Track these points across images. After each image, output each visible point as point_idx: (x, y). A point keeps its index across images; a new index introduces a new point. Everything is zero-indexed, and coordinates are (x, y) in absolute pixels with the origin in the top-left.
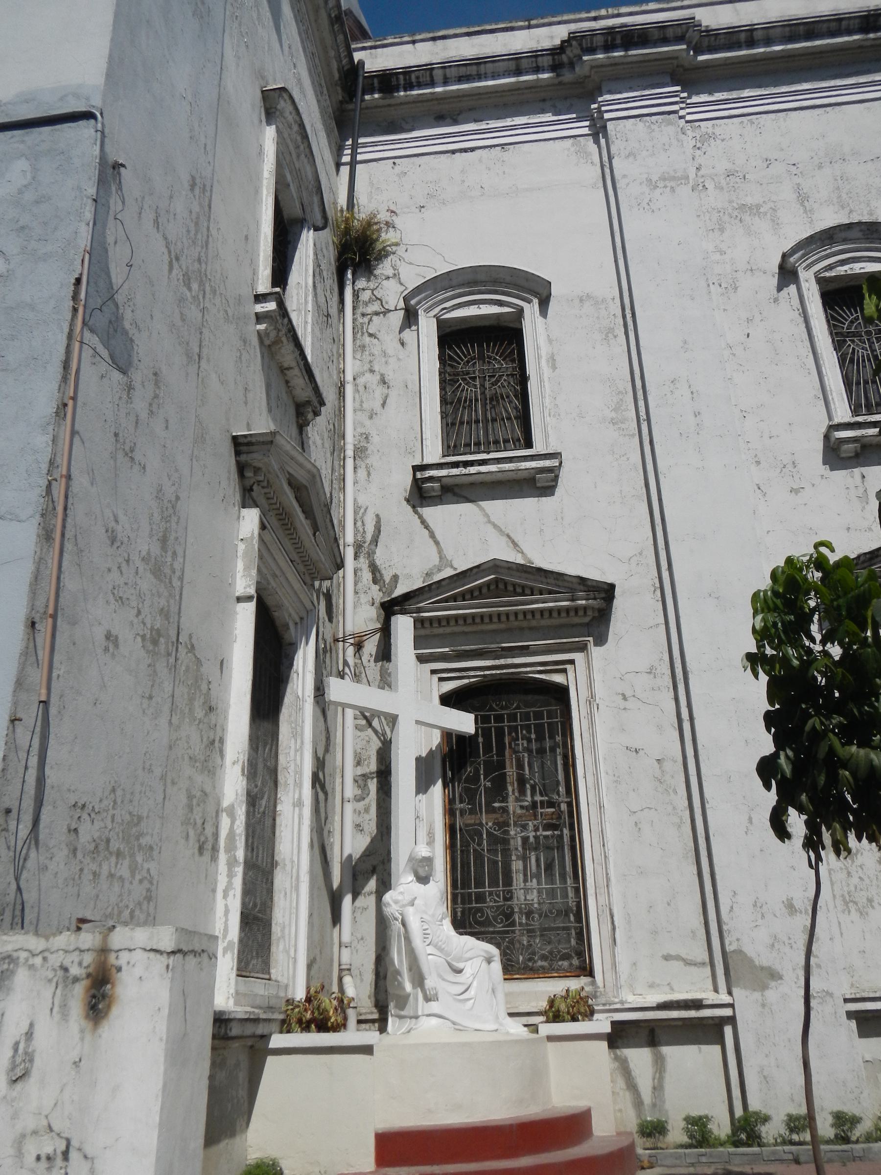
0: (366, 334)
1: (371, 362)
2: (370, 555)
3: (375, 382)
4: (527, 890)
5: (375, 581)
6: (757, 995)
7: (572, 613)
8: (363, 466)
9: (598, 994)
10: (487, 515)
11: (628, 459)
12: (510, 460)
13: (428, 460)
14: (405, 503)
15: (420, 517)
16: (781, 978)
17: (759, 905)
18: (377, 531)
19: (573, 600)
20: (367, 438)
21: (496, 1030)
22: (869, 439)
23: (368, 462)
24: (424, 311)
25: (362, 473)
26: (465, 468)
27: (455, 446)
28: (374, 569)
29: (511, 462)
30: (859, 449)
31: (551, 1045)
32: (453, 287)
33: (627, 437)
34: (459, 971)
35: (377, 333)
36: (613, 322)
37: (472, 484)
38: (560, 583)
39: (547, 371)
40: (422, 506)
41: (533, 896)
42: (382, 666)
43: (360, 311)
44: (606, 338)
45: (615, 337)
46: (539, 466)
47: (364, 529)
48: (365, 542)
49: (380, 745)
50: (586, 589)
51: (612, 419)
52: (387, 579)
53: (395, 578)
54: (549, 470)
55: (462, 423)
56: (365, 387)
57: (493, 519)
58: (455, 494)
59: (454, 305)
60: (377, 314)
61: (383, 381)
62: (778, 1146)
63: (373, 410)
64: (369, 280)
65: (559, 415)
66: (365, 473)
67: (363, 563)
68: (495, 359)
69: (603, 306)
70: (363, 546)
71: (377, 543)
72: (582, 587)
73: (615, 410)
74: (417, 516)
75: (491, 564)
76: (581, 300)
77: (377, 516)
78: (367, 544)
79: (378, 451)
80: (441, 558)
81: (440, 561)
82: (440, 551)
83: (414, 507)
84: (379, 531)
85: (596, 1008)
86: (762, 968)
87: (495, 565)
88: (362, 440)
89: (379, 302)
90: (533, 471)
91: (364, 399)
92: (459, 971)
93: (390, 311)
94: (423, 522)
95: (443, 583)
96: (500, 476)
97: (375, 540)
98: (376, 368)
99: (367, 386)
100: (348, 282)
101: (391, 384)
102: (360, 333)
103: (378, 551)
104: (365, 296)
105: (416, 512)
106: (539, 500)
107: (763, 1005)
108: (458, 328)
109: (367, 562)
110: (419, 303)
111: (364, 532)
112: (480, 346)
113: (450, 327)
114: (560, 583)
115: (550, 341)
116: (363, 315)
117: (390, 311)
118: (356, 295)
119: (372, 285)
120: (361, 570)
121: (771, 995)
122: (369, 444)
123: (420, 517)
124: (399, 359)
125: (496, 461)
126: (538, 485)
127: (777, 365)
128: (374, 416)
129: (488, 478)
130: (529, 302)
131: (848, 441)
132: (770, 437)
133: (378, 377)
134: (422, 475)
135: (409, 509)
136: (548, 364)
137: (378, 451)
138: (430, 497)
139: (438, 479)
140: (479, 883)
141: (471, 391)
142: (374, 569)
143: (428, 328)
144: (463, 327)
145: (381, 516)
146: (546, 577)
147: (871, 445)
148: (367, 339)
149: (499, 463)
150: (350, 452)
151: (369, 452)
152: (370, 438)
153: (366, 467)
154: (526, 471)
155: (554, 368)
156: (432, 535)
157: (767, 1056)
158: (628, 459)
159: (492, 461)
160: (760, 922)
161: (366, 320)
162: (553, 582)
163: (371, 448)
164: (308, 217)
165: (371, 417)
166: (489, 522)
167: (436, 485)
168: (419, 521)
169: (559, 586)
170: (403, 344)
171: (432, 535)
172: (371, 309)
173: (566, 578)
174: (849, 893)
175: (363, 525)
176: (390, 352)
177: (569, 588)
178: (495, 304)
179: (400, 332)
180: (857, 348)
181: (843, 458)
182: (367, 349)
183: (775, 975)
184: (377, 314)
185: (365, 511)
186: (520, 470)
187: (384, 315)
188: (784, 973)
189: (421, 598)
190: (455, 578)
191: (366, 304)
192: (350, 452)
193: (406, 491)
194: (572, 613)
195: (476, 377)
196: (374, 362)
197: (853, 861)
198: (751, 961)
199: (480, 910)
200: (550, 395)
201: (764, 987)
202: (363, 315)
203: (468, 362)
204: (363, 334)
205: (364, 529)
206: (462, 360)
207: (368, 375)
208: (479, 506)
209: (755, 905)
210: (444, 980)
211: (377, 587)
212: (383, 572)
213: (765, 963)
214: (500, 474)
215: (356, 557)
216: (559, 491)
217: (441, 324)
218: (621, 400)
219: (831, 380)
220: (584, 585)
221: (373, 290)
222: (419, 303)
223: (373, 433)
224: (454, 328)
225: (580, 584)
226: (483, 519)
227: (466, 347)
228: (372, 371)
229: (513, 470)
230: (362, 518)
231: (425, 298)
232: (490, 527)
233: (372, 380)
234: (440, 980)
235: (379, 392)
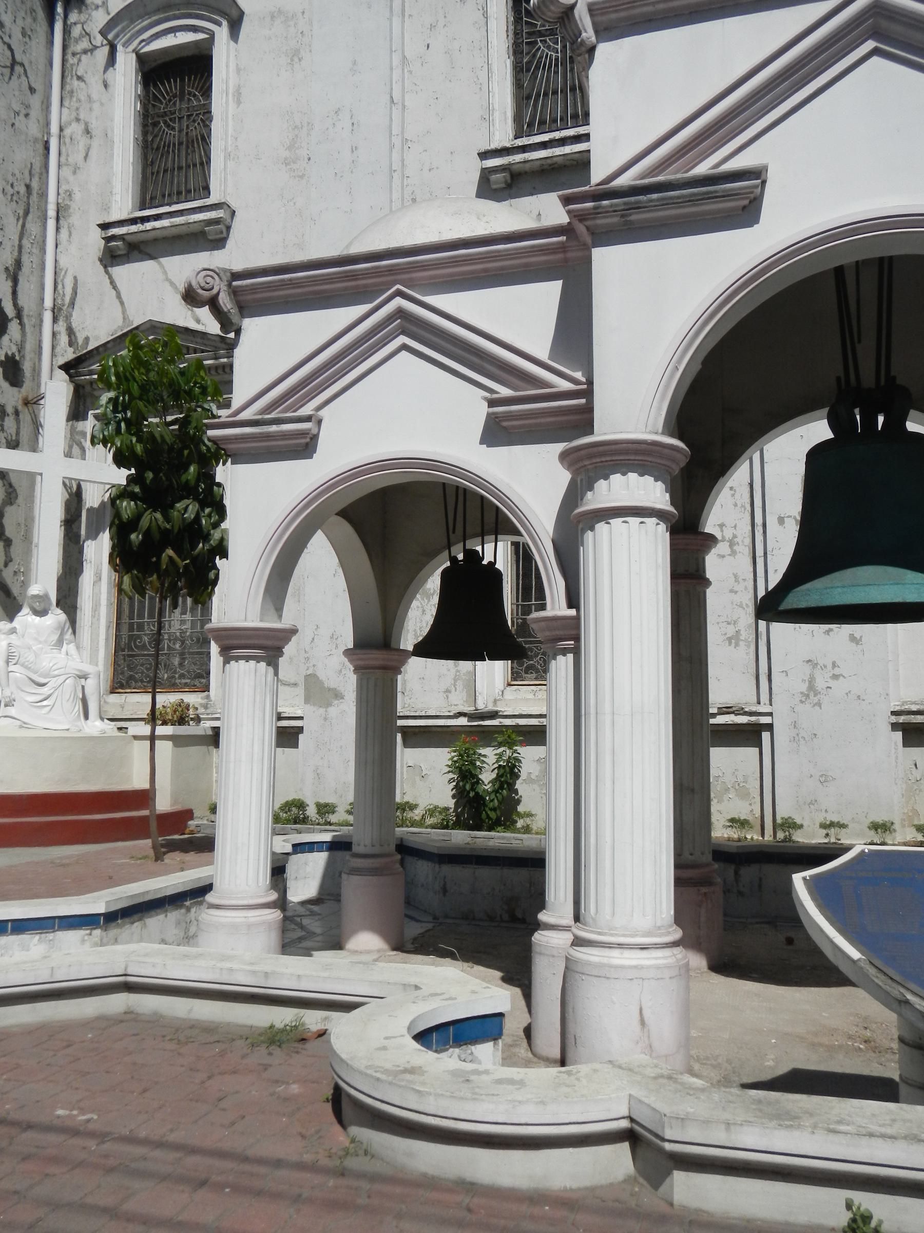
0: (75, 78)
1: (77, 109)
2: (68, 318)
3: (80, 132)
4: (183, 622)
5: (71, 344)
6: (322, 711)
7: (220, 371)
8: (66, 226)
9: (209, 706)
10: (165, 273)
11: (295, 203)
12: (181, 213)
13: (115, 216)
14: (99, 263)
15: (110, 277)
16: (342, 698)
17: (335, 637)
18: (74, 293)
19: (216, 358)
20: (70, 195)
21: (68, 730)
22: (518, 166)
23: (70, 222)
24: (123, 46)
25: (64, 233)
26: (143, 224)
27: (169, 195)
28: (70, 332)
29: (182, 215)
30: (509, 178)
31: (136, 742)
32: (149, 14)
33: (297, 179)
34: (43, 685)
35: (85, 75)
36: (300, 41)
37: (156, 240)
38: (205, 342)
39: (232, 106)
40: (112, 266)
41: (188, 625)
42: (72, 425)
43: (69, 51)
44: (291, 64)
45: (300, 60)
46: (205, 218)
47: (63, 292)
48: (64, 306)
49: (68, 496)
50: (227, 347)
51: (286, 159)
52: (80, 341)
53: (87, 339)
54: (217, 221)
55: (165, 171)
56: (71, 139)
57: (170, 276)
58: (141, 252)
59: (152, 36)
60: (85, 52)
61: (87, 131)
62: (298, 823)
63: (76, 164)
64: (80, 12)
65: (238, 158)
66: (67, 233)
67: (61, 327)
68: (195, 95)
69: (292, 23)
70: (62, 309)
71: (74, 305)
72: (223, 346)
73: (290, 148)
74: (107, 276)
75: (148, 325)
76: (273, 17)
77: (75, 278)
78: (66, 307)
79: (79, 209)
80: (124, 318)
81: (124, 322)
82: (124, 312)
83: (105, 267)
84: (76, 294)
85: (201, 716)
86: (329, 689)
87: (152, 327)
88: (66, 198)
89: (88, 37)
90: (202, 224)
91: (70, 153)
92: (43, 685)
93: (98, 47)
94: (112, 283)
95: (109, 345)
96: (175, 231)
97: (72, 304)
98: (82, 117)
99: (73, 137)
100: (57, 17)
101: (94, 134)
102: (70, 77)
103: (74, 314)
104: (76, 31)
105: (107, 272)
106: (211, 254)
107: (325, 719)
108: (163, 60)
109: (65, 325)
110: (117, 36)
111: (64, 295)
112: (182, 80)
113: (155, 60)
114: (205, 342)
115: (238, 70)
116: (74, 54)
117: (96, 47)
118: (66, 31)
119: (83, 17)
120: (60, 333)
121: (333, 711)
122: (72, 202)
123: (110, 277)
124: (102, 104)
125: (168, 215)
126: (210, 238)
127: (450, 81)
128: (77, 171)
129: (165, 233)
130: (219, 24)
131: (497, 171)
132: (430, 170)
133: (83, 126)
134: (106, 234)
135: (102, 268)
136: (234, 99)
137: (79, 209)
138: (120, 256)
139: (121, 237)
140: (141, 616)
141: (172, 136)
142: (70, 332)
143: (126, 63)
144: (167, 59)
145: (78, 278)
146: (194, 336)
147: (526, 173)
148: (76, 83)
149: (172, 217)
150: (51, 213)
151: (71, 210)
152: (73, 195)
153: (69, 227)
154: (195, 224)
155: (239, 102)
156: (119, 296)
157: (322, 758)
158: (295, 203)
159: (164, 216)
160: (334, 651)
161: (75, 60)
162: (199, 340)
163: (73, 205)
165: (74, 173)
166: (167, 279)
167: (119, 243)
168: (108, 281)
169: (205, 345)
170: (106, 86)
171: (119, 296)
172: (80, 47)
173: (209, 337)
174: (420, 628)
175: (64, 287)
176: (95, 96)
177: (213, 346)
178: (190, 30)
179: (105, 72)
180: (547, 51)
181: (496, 190)
182: (75, 94)
183: (338, 695)
184: (85, 52)
185: (66, 273)
186: (189, 223)
187: (92, 54)
188: (346, 694)
189: (92, 361)
190: (118, 341)
191: (77, 41)
192: (51, 213)
193: (100, 250)
194: (220, 371)
195: (175, 118)
196: (81, 110)
197: (429, 601)
198: (322, 683)
199: (139, 637)
200: (232, 136)
201: (329, 705)
202: (74, 54)
203: (170, 101)
204: (72, 76)
205: (63, 292)
206: (165, 98)
207: (74, 125)
208: (160, 263)
209: (332, 638)
210: (23, 691)
211: (72, 350)
212: (78, 334)
213: (332, 685)
214: (154, 233)
215: (55, 320)
216: (230, 243)
217: (142, 59)
218: (297, 136)
219: (497, 95)
220: (225, 343)
221: (83, 25)
222: (117, 36)
223: (76, 190)
224: (159, 62)
225: (221, 342)
226: (161, 277)
227: (169, 83)
228: (78, 120)
229: (183, 224)
230: (62, 281)
231: (123, 30)
232: (167, 284)
233: (75, 129)
234: (19, 691)
235: (83, 142)
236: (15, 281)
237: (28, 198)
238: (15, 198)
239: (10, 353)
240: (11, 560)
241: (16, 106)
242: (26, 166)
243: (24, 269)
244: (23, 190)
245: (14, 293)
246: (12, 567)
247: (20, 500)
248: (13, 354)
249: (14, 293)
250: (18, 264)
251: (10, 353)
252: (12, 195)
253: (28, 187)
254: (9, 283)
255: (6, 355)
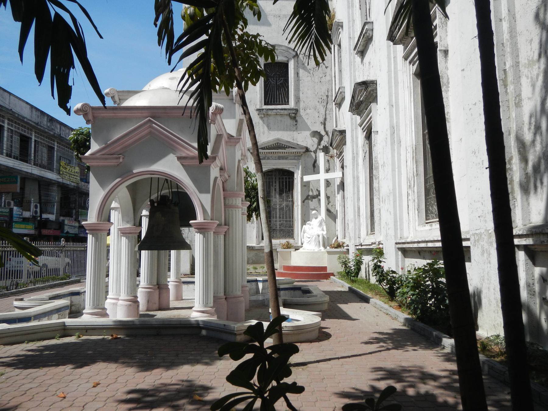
164: (290, 58)
236: (325, 124)
237: (327, 99)
238: (322, 102)
239: (324, 145)
240: (330, 202)
241: (321, 76)
242: (326, 90)
243: (327, 120)
244: (325, 98)
245: (325, 128)
246: (330, 204)
247: (332, 185)
248: (326, 145)
249: (325, 128)
250: (325, 119)
251: (324, 145)
252: (322, 101)
253: (327, 96)
254: (323, 126)
255: (323, 146)
